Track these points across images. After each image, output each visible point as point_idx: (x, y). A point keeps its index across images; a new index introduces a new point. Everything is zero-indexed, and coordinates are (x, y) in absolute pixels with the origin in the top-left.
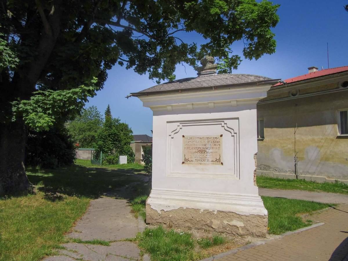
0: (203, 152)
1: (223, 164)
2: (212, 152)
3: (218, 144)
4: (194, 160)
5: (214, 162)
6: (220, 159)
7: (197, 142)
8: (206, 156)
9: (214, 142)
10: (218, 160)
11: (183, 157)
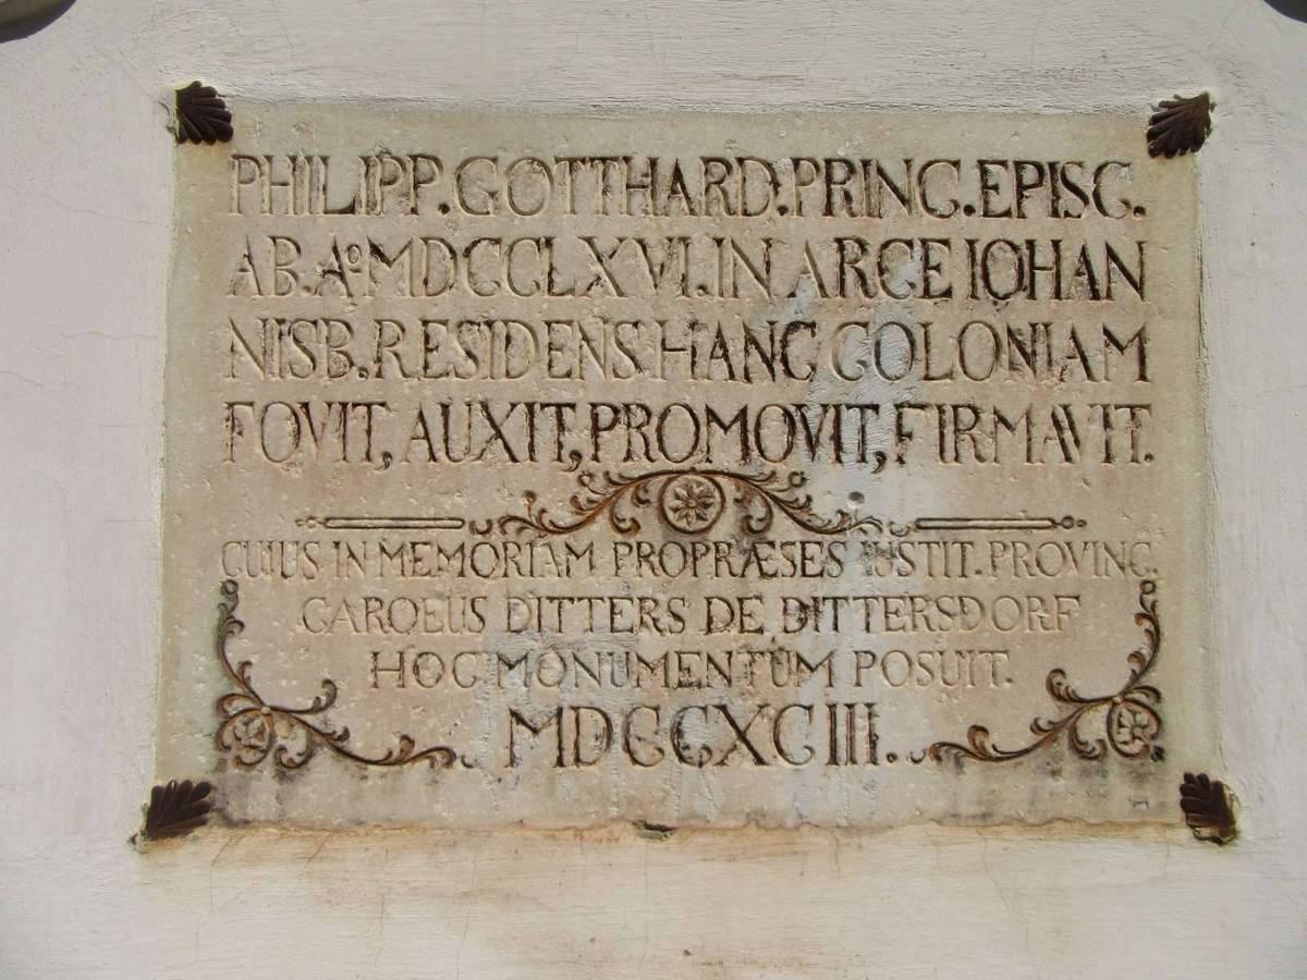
0: (725, 529)
1: (1242, 822)
2: (960, 523)
3: (1094, 343)
4: (483, 738)
5: (1015, 787)
6: (1141, 692)
7: (574, 263)
8: (808, 610)
9: (1004, 278)
10: (1093, 727)
11: (171, 659)
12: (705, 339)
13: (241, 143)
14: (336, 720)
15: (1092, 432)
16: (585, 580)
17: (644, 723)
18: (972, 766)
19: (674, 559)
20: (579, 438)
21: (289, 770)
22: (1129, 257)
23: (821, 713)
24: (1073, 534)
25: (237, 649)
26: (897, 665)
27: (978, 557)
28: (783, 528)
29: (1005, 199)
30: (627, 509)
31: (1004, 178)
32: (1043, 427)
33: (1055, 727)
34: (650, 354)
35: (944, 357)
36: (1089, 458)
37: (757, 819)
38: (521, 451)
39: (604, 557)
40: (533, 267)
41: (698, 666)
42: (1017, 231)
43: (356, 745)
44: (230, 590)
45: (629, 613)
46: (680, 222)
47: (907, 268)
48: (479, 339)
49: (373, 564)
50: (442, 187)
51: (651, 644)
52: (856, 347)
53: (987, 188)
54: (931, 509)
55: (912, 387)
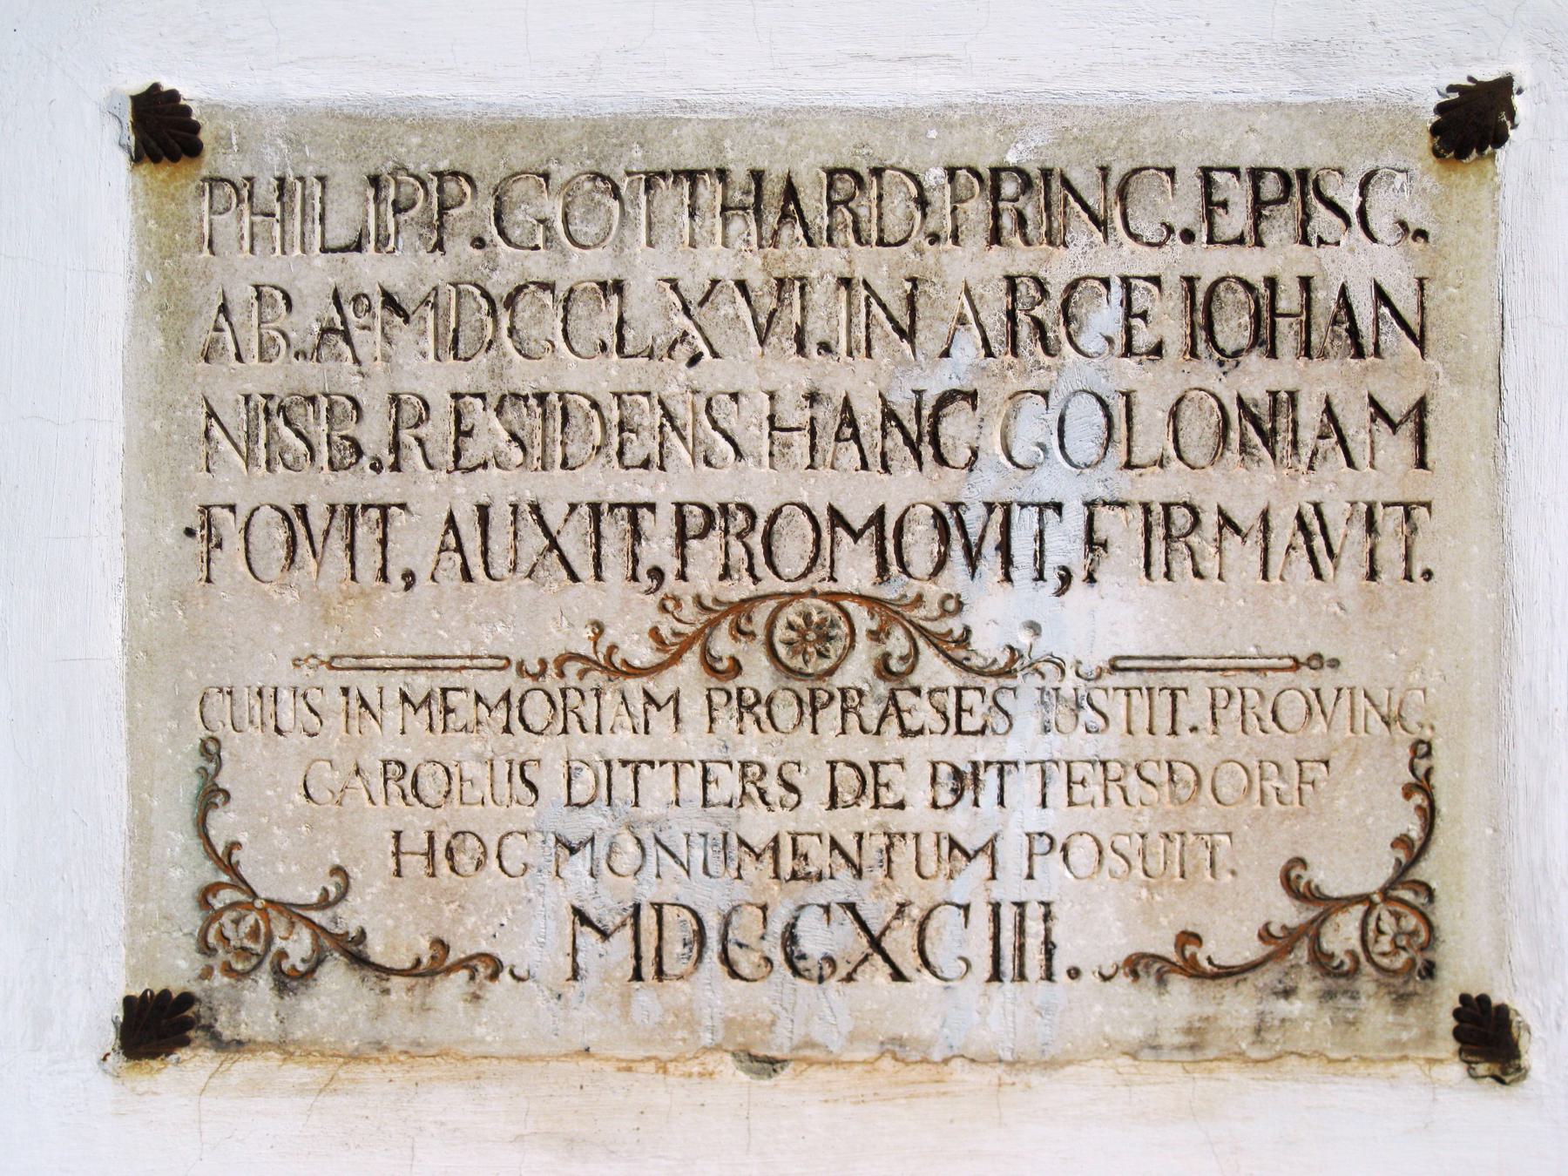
0: (857, 671)
1: (1532, 1054)
2: (1171, 663)
3: (1355, 419)
8: (964, 781)
9: (1233, 328)
10: (1342, 936)
11: (141, 834)
12: (827, 416)
13: (215, 160)
14: (349, 918)
15: (1350, 538)
16: (663, 739)
17: (746, 926)
18: (1180, 985)
19: (786, 713)
20: (659, 548)
21: (288, 981)
22: (1406, 303)
23: (981, 915)
24: (1327, 680)
25: (223, 824)
26: (1083, 852)
27: (1194, 709)
28: (933, 670)
29: (1235, 220)
30: (723, 644)
31: (1236, 193)
32: (1284, 530)
33: (1292, 936)
34: (756, 439)
35: (1152, 438)
36: (1350, 574)
37: (896, 1048)
38: (585, 570)
39: (694, 707)
40: (598, 322)
41: (820, 856)
42: (1252, 264)
43: (376, 950)
44: (210, 750)
45: (728, 784)
46: (794, 254)
47: (1103, 317)
48: (528, 420)
49: (394, 714)
50: (474, 211)
51: (759, 825)
52: (1033, 426)
53: (1212, 206)
54: (1130, 644)
55: (1111, 480)
